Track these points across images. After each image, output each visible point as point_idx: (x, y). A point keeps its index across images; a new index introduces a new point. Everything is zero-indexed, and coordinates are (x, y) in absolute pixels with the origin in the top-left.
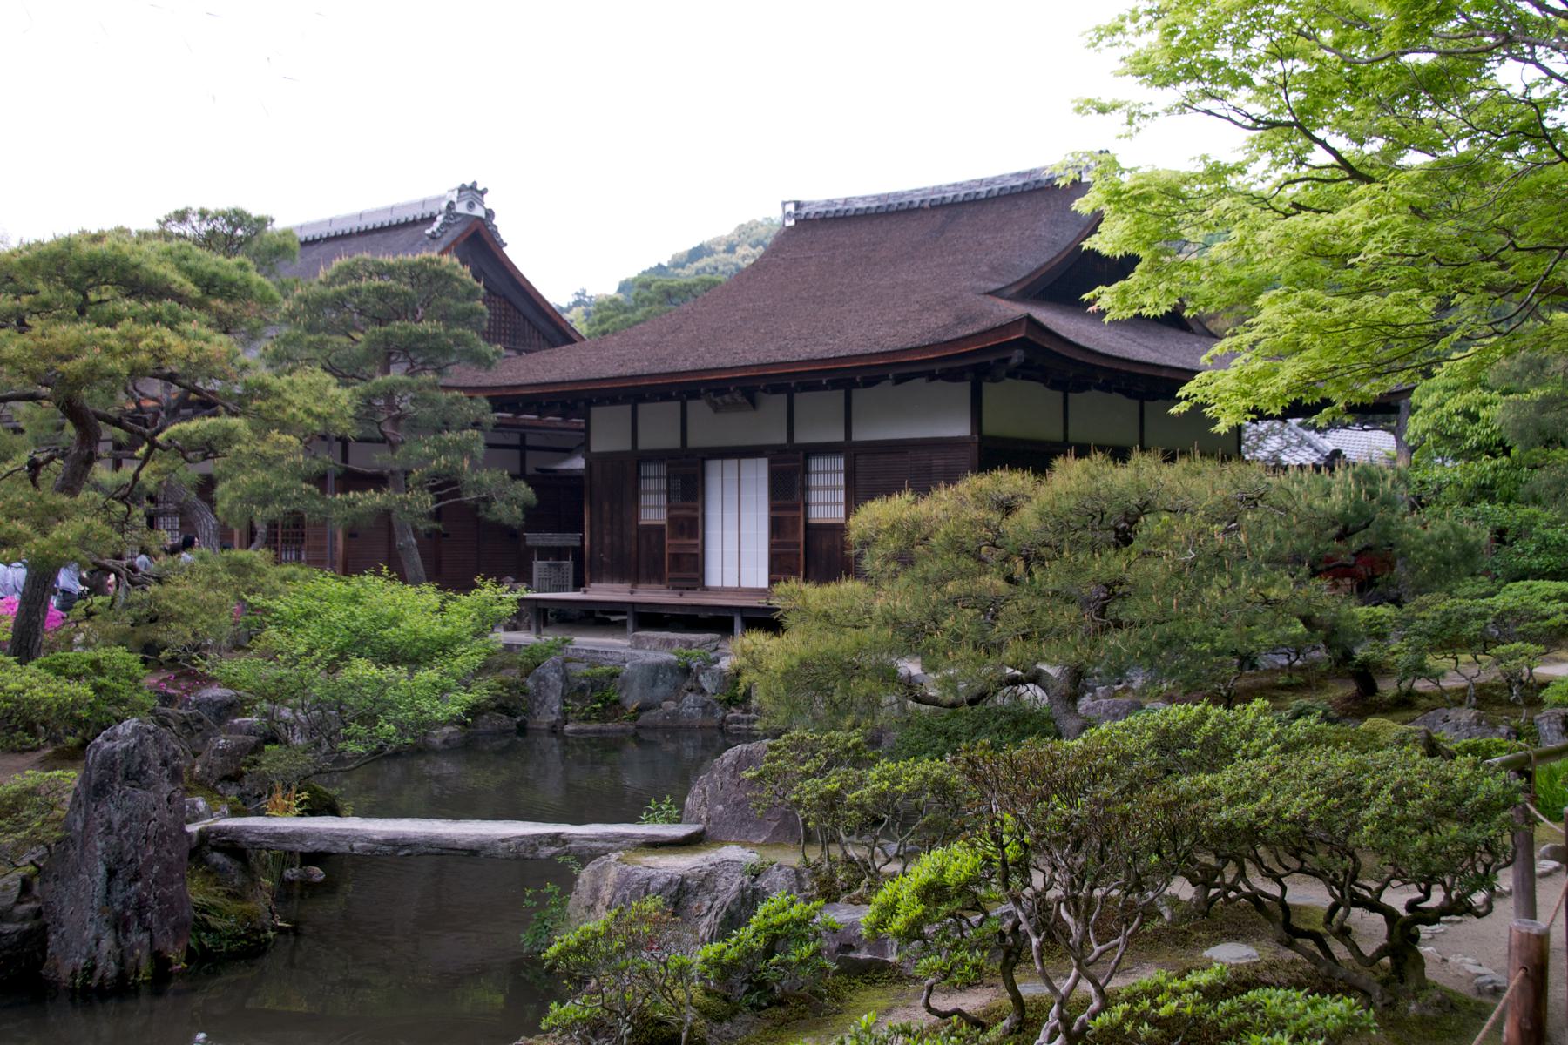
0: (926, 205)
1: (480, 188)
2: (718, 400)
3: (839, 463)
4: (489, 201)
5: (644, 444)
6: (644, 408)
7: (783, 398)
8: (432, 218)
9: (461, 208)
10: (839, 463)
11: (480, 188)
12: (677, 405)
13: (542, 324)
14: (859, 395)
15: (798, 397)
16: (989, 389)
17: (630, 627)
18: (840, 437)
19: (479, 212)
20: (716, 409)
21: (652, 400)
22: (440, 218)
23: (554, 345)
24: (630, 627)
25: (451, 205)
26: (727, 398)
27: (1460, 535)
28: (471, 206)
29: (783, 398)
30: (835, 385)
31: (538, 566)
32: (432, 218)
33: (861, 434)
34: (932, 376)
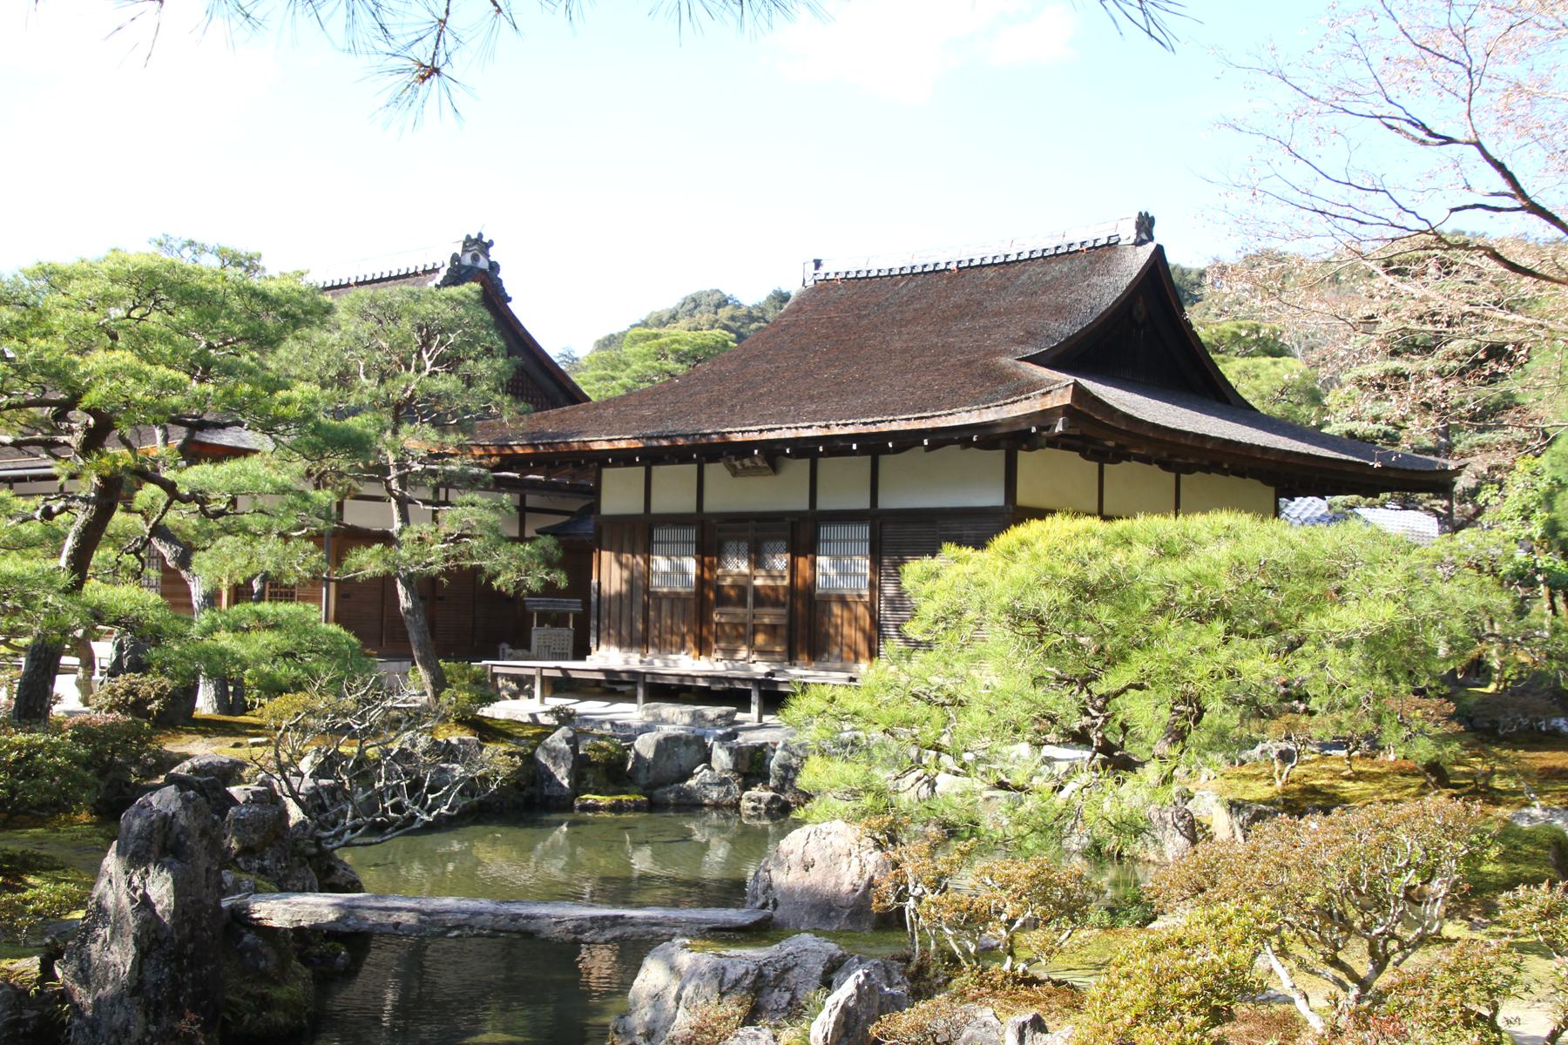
0: (953, 266)
1: (485, 240)
2: (737, 463)
3: (864, 531)
4: (494, 254)
5: (658, 507)
6: (658, 471)
7: (806, 462)
8: (435, 270)
9: (467, 260)
10: (864, 531)
11: (485, 240)
12: (694, 467)
13: (546, 382)
14: (886, 462)
15: (822, 462)
16: (1025, 459)
17: (640, 698)
18: (864, 503)
19: (483, 264)
20: (735, 473)
21: (615, 464)
22: (443, 272)
23: (555, 405)
24: (640, 698)
25: (455, 258)
26: (747, 462)
27: (1557, 680)
28: (475, 258)
29: (806, 462)
30: (862, 451)
31: (537, 635)
32: (435, 270)
33: (887, 502)
34: (966, 443)
